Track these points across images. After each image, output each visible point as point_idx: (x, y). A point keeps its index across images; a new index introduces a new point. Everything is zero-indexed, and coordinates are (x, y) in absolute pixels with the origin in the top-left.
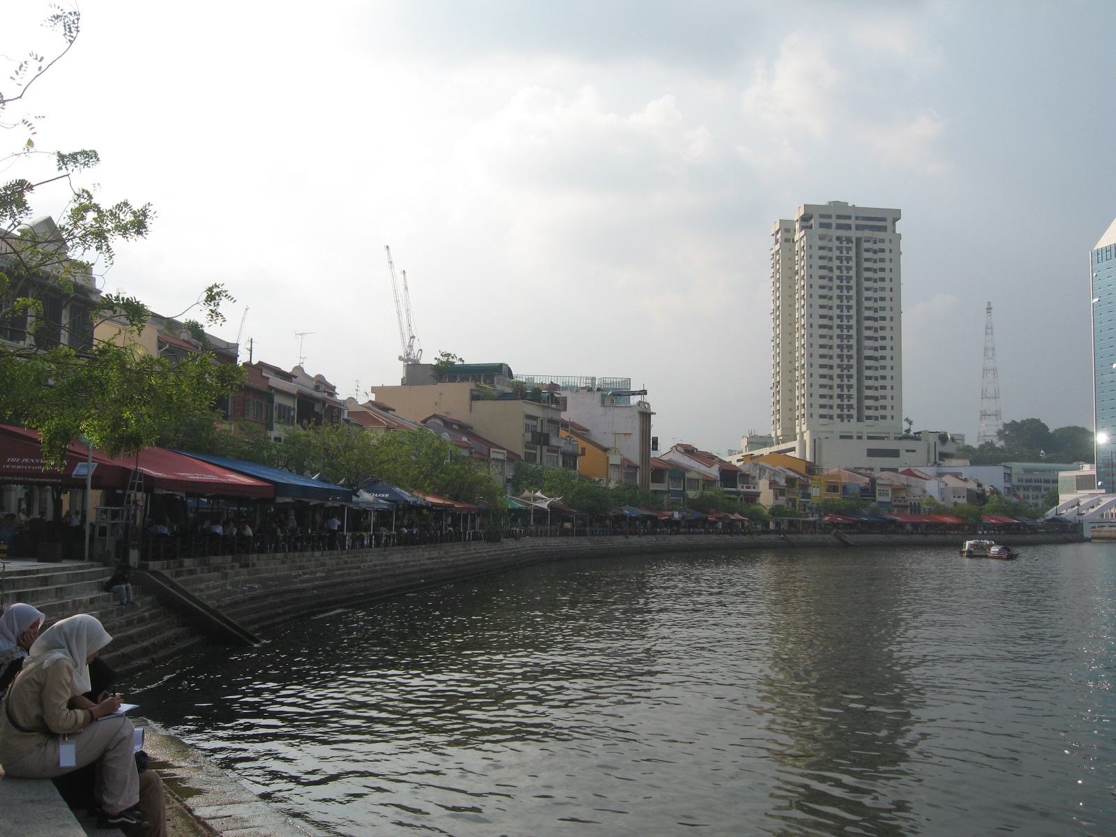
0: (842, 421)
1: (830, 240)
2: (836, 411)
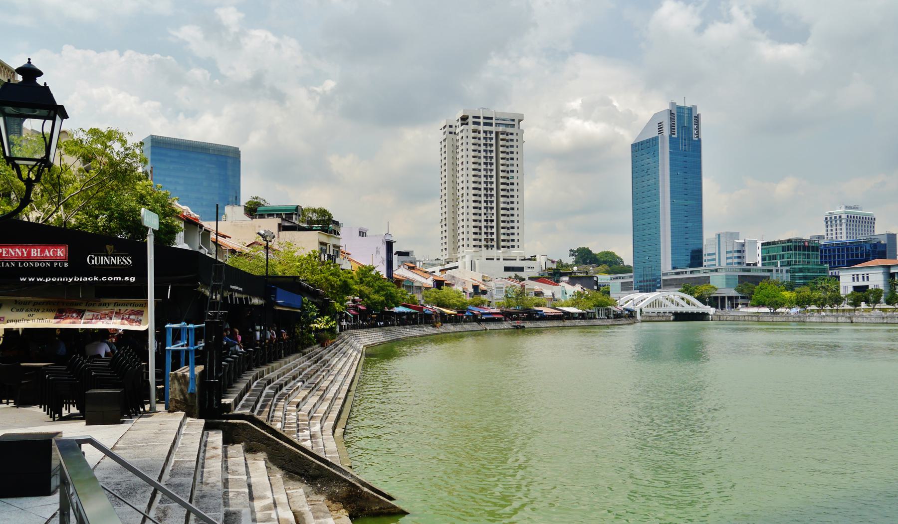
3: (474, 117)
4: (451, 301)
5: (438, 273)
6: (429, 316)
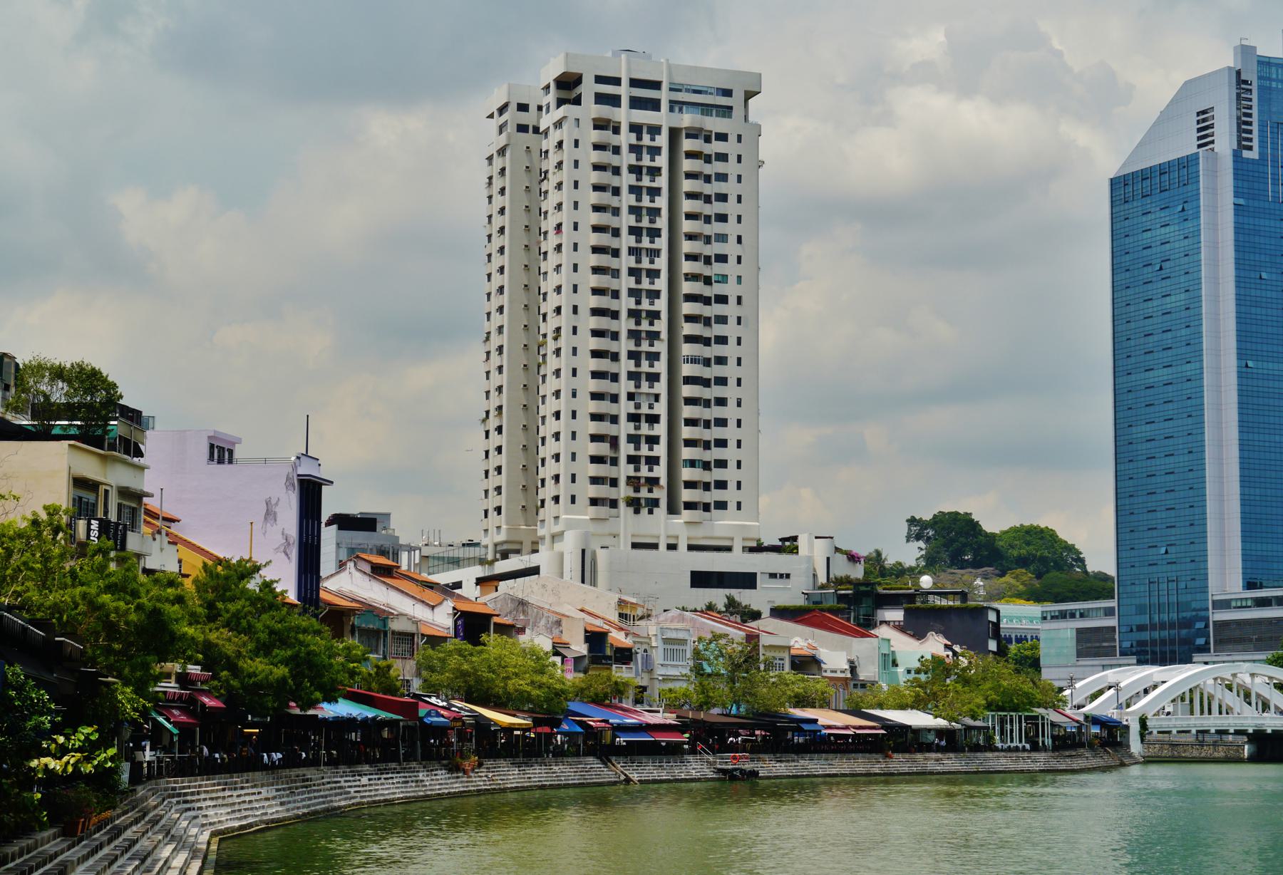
0: (637, 512)
1: (616, 130)
2: (624, 491)
3: (600, 80)
5: (470, 590)
6: (440, 731)
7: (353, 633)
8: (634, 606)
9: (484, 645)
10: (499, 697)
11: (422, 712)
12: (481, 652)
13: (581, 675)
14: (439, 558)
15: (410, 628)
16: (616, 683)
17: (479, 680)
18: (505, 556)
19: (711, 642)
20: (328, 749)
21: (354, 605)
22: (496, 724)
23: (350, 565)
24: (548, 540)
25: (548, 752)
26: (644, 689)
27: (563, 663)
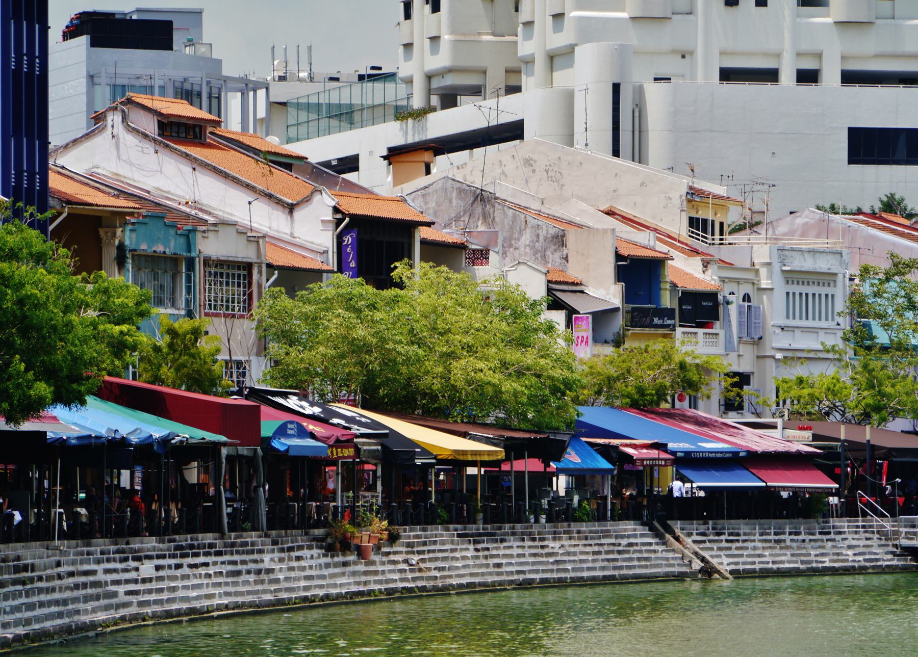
4: (460, 370)
5: (374, 175)
6: (308, 469)
7: (121, 262)
8: (721, 202)
9: (401, 285)
10: (434, 397)
11: (267, 428)
12: (395, 301)
13: (609, 350)
14: (308, 107)
15: (242, 252)
16: (682, 366)
17: (389, 362)
18: (449, 99)
19: (888, 280)
20: (69, 501)
21: (122, 202)
22: (425, 452)
23: (114, 119)
24: (540, 64)
25: (536, 510)
26: (743, 379)
27: (569, 323)
